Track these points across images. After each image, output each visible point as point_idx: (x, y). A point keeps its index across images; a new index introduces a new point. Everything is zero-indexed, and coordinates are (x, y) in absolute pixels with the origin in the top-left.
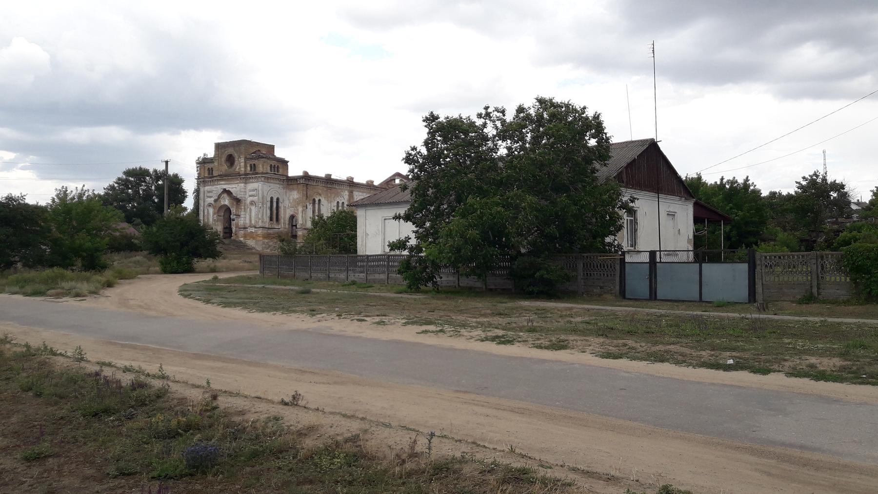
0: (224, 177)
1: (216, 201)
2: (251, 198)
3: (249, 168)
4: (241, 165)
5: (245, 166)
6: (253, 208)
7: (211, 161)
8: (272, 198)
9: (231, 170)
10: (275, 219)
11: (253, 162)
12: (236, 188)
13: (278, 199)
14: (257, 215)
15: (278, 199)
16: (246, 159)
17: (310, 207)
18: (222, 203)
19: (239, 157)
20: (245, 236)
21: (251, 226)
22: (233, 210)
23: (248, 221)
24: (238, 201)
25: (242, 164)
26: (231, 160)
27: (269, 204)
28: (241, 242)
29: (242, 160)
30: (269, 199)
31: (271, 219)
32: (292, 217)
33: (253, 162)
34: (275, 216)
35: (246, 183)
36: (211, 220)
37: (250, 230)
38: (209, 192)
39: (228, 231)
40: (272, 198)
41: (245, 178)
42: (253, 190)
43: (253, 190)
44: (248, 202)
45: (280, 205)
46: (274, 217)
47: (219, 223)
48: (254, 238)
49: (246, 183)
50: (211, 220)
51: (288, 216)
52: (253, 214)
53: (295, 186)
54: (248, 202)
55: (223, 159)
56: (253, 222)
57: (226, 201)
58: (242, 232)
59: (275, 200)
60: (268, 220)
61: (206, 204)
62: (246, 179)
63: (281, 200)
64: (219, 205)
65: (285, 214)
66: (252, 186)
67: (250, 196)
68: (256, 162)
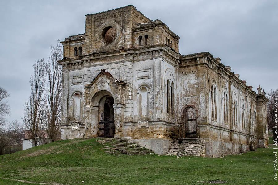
0: (98, 56)
1: (88, 87)
2: (142, 81)
3: (137, 42)
5: (133, 39)
6: (144, 95)
7: (80, 38)
8: (168, 81)
9: (110, 46)
11: (143, 34)
12: (118, 68)
13: (173, 83)
15: (173, 83)
16: (134, 30)
18: (99, 88)
19: (123, 28)
23: (136, 113)
25: (129, 37)
33: (143, 34)
35: (133, 61)
36: (77, 113)
38: (76, 77)
39: (107, 127)
40: (168, 81)
41: (133, 54)
42: (146, 70)
43: (146, 70)
47: (93, 116)
48: (147, 136)
49: (133, 61)
50: (77, 113)
52: (144, 103)
54: (137, 84)
55: (98, 35)
56: (144, 114)
57: (106, 86)
58: (128, 129)
61: (71, 92)
62: (134, 55)
66: (141, 64)
67: (140, 78)
68: (149, 32)
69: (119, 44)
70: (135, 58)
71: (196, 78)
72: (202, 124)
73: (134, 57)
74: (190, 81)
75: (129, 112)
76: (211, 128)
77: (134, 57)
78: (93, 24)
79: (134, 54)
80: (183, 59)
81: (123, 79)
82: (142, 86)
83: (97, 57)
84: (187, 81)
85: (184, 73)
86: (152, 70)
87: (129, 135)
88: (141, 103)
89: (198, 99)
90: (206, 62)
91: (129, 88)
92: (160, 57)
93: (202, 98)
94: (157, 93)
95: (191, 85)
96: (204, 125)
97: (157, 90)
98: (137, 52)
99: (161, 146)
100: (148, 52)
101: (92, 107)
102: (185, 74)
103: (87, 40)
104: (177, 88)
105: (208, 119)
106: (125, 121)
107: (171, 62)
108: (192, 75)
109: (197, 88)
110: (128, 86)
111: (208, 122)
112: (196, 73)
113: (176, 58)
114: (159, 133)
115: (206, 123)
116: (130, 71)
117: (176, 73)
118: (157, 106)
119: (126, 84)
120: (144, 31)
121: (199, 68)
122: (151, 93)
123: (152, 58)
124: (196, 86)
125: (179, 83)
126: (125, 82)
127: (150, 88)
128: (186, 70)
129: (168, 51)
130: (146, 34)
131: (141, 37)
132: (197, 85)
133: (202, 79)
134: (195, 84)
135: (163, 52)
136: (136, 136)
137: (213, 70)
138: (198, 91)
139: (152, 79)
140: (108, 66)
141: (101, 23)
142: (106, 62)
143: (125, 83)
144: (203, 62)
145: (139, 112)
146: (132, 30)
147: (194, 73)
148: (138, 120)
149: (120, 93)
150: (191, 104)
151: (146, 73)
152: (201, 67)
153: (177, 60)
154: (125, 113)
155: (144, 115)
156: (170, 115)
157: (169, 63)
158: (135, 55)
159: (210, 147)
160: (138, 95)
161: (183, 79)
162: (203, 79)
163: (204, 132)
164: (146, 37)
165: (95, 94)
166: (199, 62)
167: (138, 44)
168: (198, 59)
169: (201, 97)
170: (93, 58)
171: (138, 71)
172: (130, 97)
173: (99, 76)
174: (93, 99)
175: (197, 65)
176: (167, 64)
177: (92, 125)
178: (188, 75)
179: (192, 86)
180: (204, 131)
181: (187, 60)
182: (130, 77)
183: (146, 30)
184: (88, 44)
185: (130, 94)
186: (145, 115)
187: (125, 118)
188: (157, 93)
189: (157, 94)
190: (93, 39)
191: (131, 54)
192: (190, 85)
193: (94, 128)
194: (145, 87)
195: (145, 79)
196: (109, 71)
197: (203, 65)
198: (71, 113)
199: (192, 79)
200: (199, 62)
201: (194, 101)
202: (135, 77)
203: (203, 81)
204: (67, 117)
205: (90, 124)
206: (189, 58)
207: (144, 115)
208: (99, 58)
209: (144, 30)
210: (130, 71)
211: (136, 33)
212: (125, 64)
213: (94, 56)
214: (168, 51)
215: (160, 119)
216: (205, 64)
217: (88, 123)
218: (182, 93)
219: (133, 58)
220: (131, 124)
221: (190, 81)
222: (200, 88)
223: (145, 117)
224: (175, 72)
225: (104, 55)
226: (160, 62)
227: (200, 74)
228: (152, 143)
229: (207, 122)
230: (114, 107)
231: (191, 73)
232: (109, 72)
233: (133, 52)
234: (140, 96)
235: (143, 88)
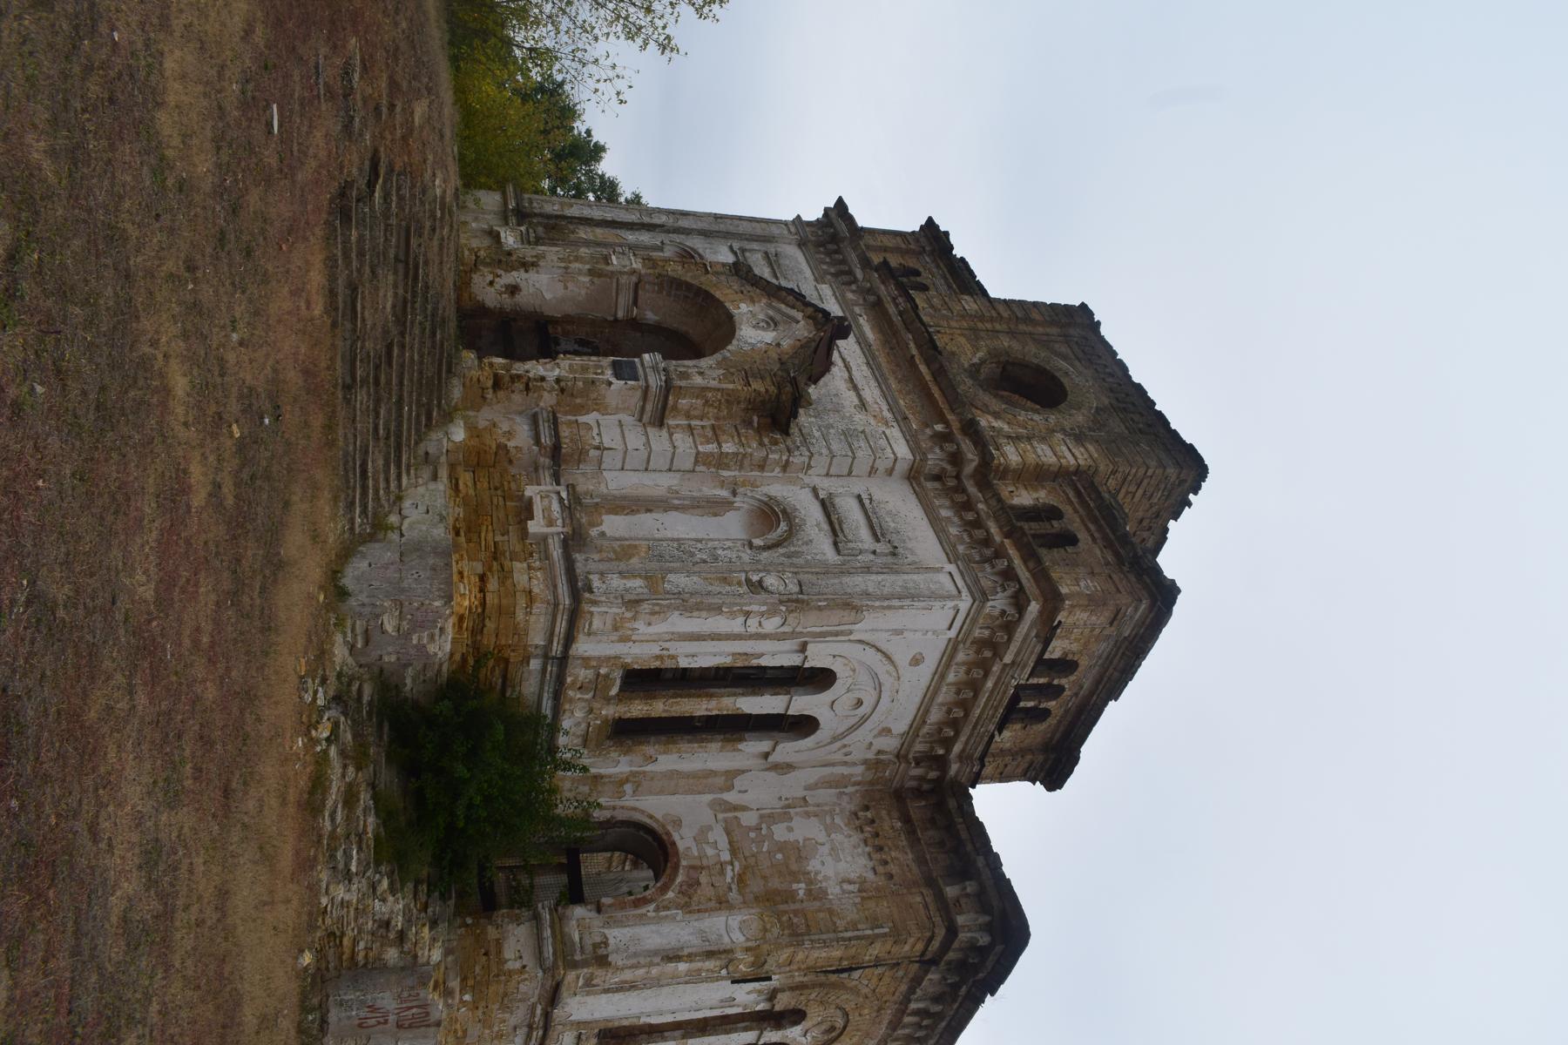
2: (811, 513)
3: (1024, 498)
4: (1032, 445)
5: (1036, 475)
6: (732, 526)
8: (821, 679)
10: (638, 709)
13: (805, 725)
14: (684, 554)
15: (805, 725)
17: (747, 997)
18: (743, 310)
19: (1079, 438)
20: (484, 460)
21: (573, 504)
22: (704, 373)
23: (616, 482)
24: (776, 408)
25: (1044, 454)
26: (1035, 387)
27: (778, 655)
28: (434, 414)
29: (1072, 455)
30: (818, 657)
31: (642, 680)
32: (651, 848)
33: (1073, 521)
34: (670, 705)
37: (543, 496)
40: (821, 679)
44: (777, 489)
45: (754, 746)
46: (659, 707)
47: (581, 287)
48: (468, 528)
49: (913, 476)
51: (653, 806)
52: (679, 526)
53: (902, 858)
56: (614, 525)
59: (802, 703)
60: (641, 652)
63: (789, 749)
64: (726, 292)
65: (669, 788)
67: (827, 506)
69: (990, 418)
70: (937, 485)
71: (846, 886)
72: (561, 939)
73: (937, 478)
74: (825, 850)
75: (619, 437)
76: (530, 1027)
77: (937, 478)
78: (1054, 330)
79: (958, 477)
80: (952, 803)
81: (804, 418)
82: (784, 511)
83: (897, 319)
84: (821, 836)
85: (869, 814)
86: (890, 559)
87: (471, 429)
88: (676, 508)
89: (722, 904)
90: (963, 936)
91: (761, 444)
92: (980, 596)
93: (732, 928)
94: (755, 578)
95: (800, 858)
96: (549, 950)
97: (771, 581)
98: (972, 489)
99: (403, 590)
100: (987, 541)
101: (634, 279)
102: (863, 820)
103: (969, 304)
104: (776, 767)
105: (589, 983)
106: (562, 418)
107: (935, 716)
108: (863, 861)
109: (791, 896)
110: (776, 443)
111: (571, 976)
112: (881, 881)
113: (957, 748)
114: (493, 585)
115: (566, 957)
116: (862, 464)
117: (865, 762)
118: (671, 577)
119: (786, 432)
120: (1092, 527)
121: (919, 899)
122: (746, 555)
123: (952, 557)
124: (801, 888)
125: (800, 793)
126: (794, 430)
127: (781, 551)
128: (890, 824)
129: (1008, 659)
130: (1082, 535)
131: (1052, 513)
132: (809, 892)
133: (852, 915)
134: (810, 882)
135: (1011, 610)
136: (465, 478)
137: (895, 1025)
138: (772, 900)
139: (830, 555)
140: (864, 368)
141: (1065, 358)
142: (882, 360)
143: (788, 426)
144: (961, 920)
145: (624, 498)
146: (1078, 471)
147: (880, 869)
148: (571, 488)
149: (731, 386)
150: (684, 863)
151: (865, 533)
152: (926, 906)
153: (941, 763)
154: (609, 421)
155: (603, 528)
156: (608, 700)
157: (940, 675)
158: (951, 483)
159: (387, 1001)
160: (724, 493)
161: (832, 813)
162: (854, 926)
163: (499, 952)
164: (1071, 540)
165: (708, 296)
166: (951, 891)
167: (1016, 501)
168: (971, 887)
169: (735, 920)
170: (892, 309)
171: (864, 496)
172: (711, 448)
173: (810, 310)
174: (677, 284)
175: (930, 882)
176: (926, 671)
177: (532, 276)
178: (856, 838)
179: (794, 867)
180: (509, 953)
181: (950, 828)
182: (825, 451)
183: (1105, 538)
184: (957, 308)
185: (729, 447)
186: (603, 534)
187: (582, 419)
188: (755, 578)
189: (748, 581)
190: (980, 325)
191: (956, 459)
192: (798, 852)
193: (513, 290)
194: (783, 526)
195: (826, 526)
196: (838, 371)
197: (937, 919)
198: (583, 233)
199: (839, 862)
200: (951, 891)
201: (704, 879)
202: (826, 486)
203: (840, 924)
204: (564, 217)
205: (534, 264)
206: (964, 835)
207: (603, 528)
208: (895, 333)
209: (1100, 529)
210: (862, 464)
211: (1071, 494)
212: (895, 433)
213: (901, 313)
214: (1008, 659)
215: (587, 595)
216: (952, 931)
217: (541, 256)
218: (744, 808)
219: (936, 471)
220: (546, 439)
221: (825, 850)
222: (796, 913)
223: (594, 532)
224: (870, 755)
225: (919, 347)
226: (950, 597)
227: (883, 908)
228: (418, 548)
229: (575, 965)
230: (646, 356)
231: (877, 856)
232: (834, 370)
233: (974, 464)
234: (716, 507)
235: (771, 515)
